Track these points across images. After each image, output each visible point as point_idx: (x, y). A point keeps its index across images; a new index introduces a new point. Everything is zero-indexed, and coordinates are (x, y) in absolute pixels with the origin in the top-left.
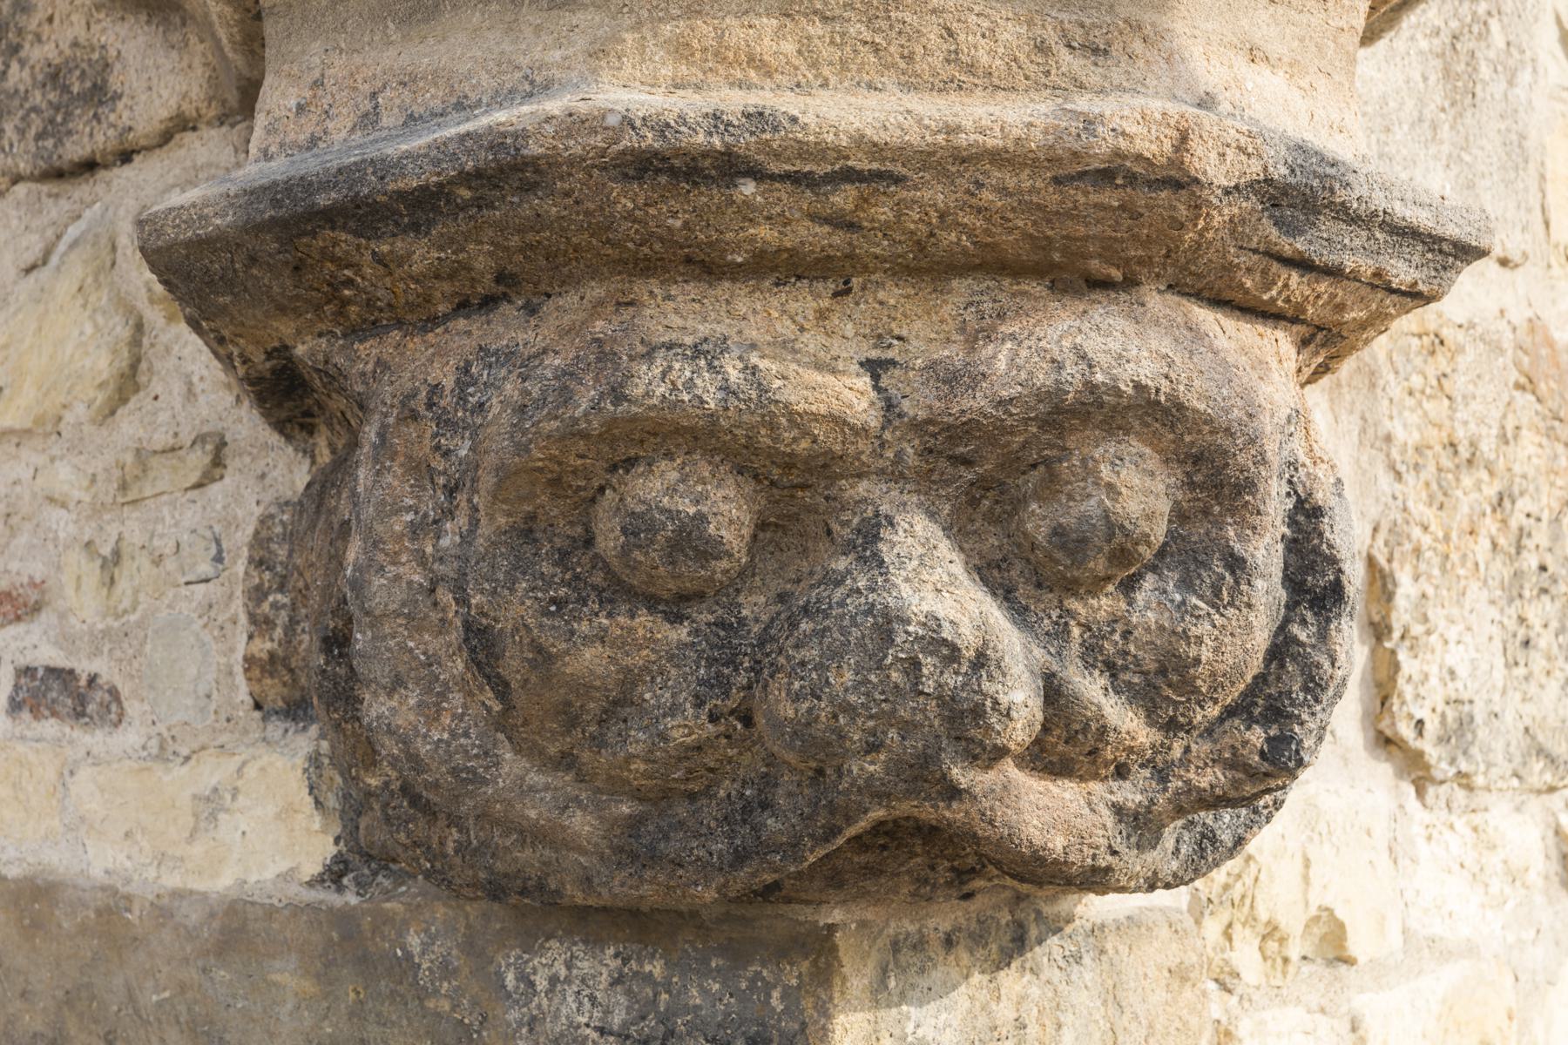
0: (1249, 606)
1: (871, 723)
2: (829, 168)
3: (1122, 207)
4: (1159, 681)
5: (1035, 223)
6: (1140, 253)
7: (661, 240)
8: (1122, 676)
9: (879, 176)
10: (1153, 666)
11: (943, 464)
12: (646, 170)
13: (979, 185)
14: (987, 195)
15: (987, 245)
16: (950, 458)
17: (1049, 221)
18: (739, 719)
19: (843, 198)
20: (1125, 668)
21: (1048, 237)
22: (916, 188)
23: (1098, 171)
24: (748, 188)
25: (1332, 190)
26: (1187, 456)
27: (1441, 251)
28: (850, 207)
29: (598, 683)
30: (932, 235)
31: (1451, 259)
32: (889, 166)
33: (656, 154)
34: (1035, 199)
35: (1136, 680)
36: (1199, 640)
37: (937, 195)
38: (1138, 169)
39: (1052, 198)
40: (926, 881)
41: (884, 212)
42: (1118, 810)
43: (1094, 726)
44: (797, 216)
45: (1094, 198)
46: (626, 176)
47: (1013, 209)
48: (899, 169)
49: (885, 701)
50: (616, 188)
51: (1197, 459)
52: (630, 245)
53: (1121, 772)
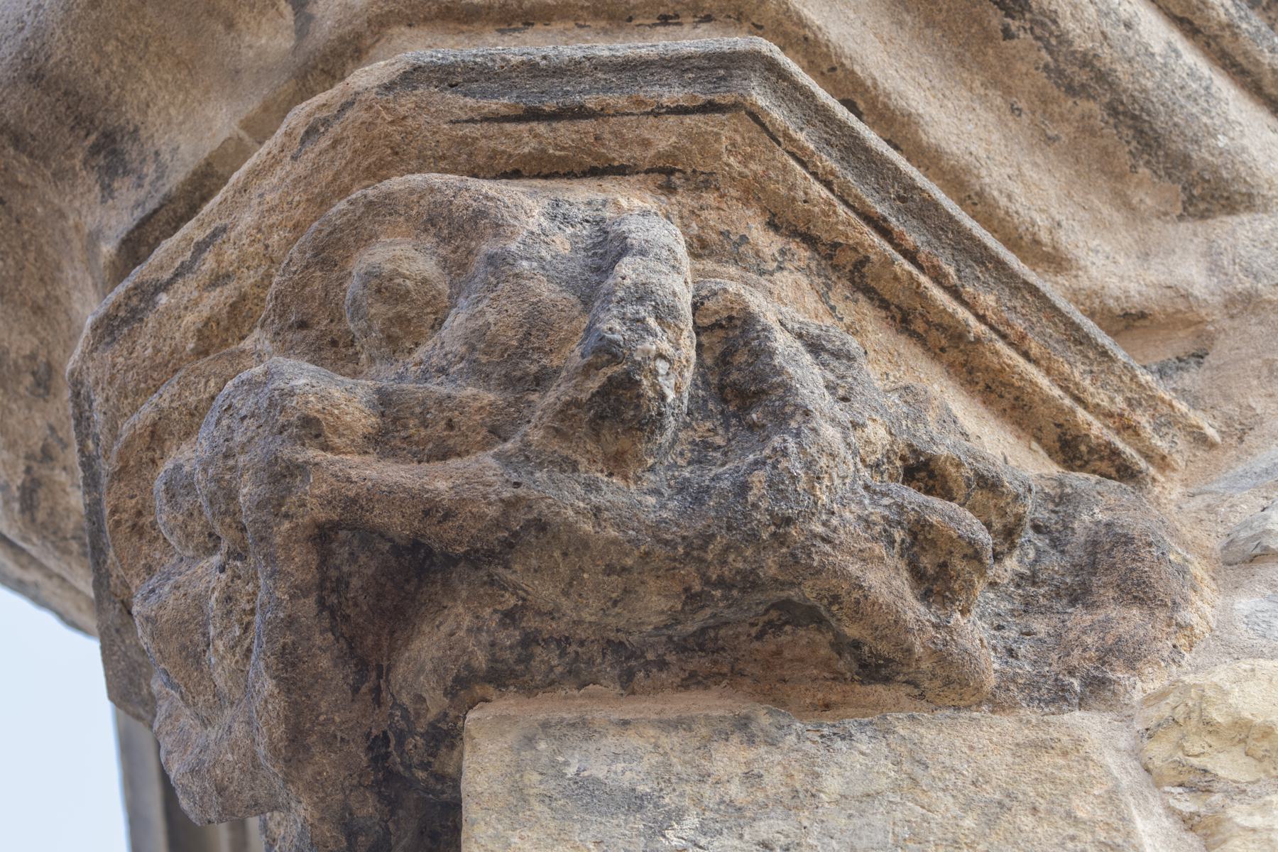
0: (517, 276)
1: (231, 462)
2: (189, 254)
3: (334, 144)
4: (477, 355)
5: (305, 191)
6: (370, 161)
7: (154, 368)
8: (451, 370)
9: (214, 235)
10: (463, 349)
11: (289, 336)
12: (112, 332)
13: (261, 196)
14: (268, 198)
15: (295, 227)
16: (290, 327)
17: (311, 184)
18: (235, 559)
19: (209, 262)
20: (450, 364)
21: (318, 194)
22: (235, 226)
23: (307, 133)
24: (163, 299)
25: (503, 59)
26: (425, 223)
27: (703, 69)
28: (214, 265)
29: (186, 617)
30: (267, 247)
31: (722, 72)
32: (214, 225)
33: (107, 316)
34: (292, 177)
35: (461, 365)
36: (482, 313)
37: (247, 219)
38: (325, 114)
39: (300, 169)
40: (479, 630)
41: (231, 254)
42: (497, 456)
43: (430, 403)
44: (196, 294)
45: (317, 150)
46: (108, 344)
47: (288, 194)
48: (218, 223)
49: (227, 440)
50: (108, 354)
51: (432, 221)
52: (142, 385)
53: (497, 433)
